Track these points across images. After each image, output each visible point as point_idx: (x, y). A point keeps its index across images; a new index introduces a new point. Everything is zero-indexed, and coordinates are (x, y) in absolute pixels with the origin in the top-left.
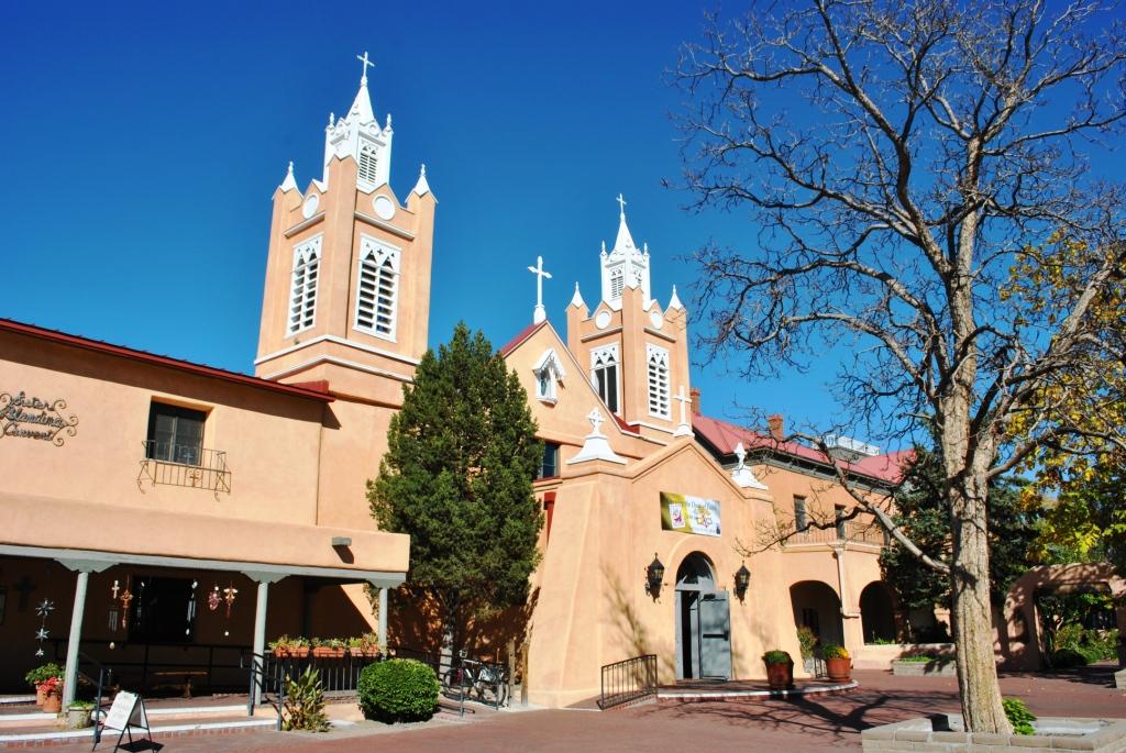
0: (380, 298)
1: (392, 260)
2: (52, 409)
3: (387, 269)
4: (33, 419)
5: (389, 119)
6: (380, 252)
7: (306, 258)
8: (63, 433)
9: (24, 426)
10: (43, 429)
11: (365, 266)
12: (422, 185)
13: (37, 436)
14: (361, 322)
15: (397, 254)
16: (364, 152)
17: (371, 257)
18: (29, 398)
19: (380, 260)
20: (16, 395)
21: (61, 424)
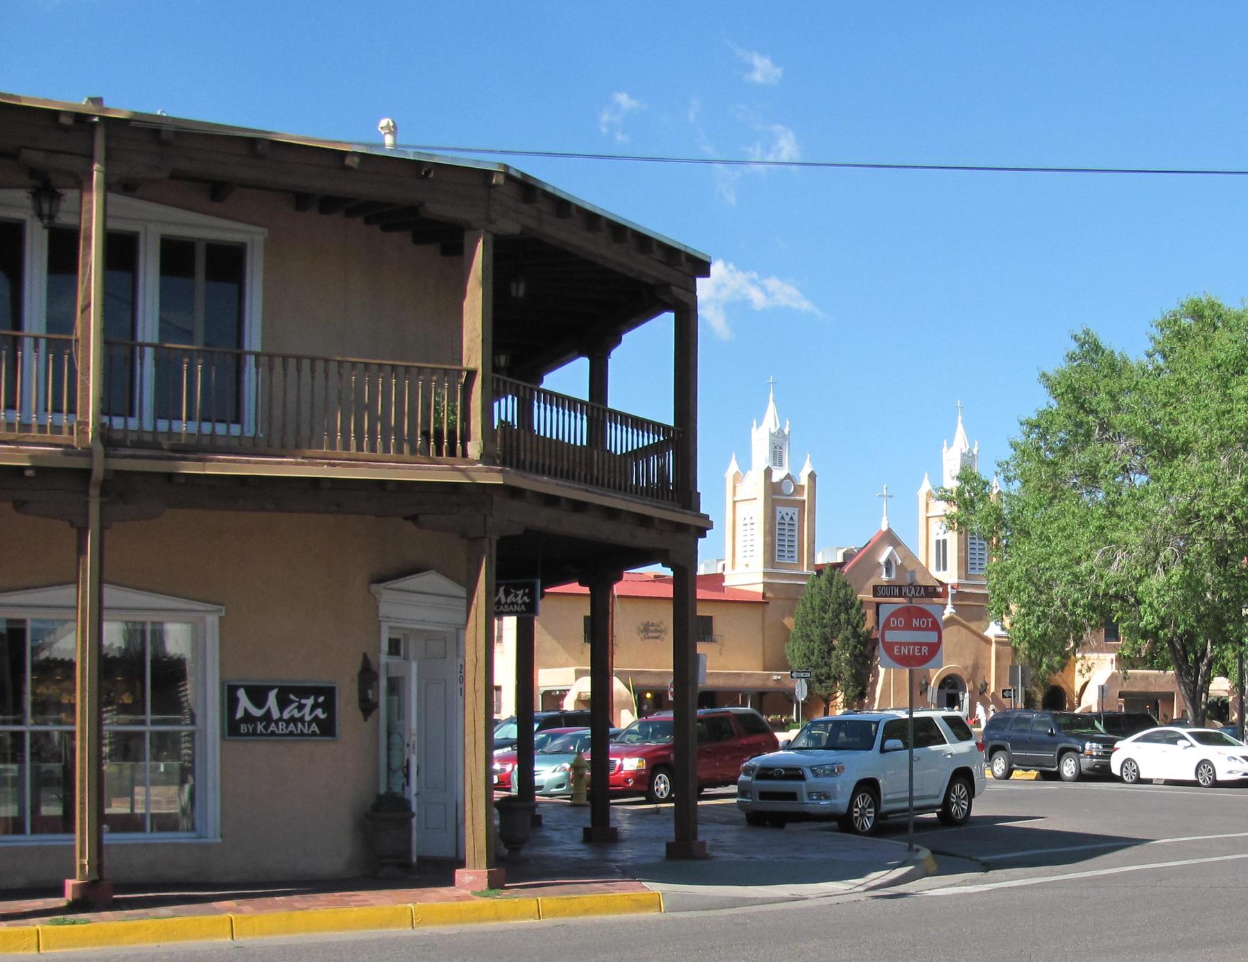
0: (788, 541)
2: (658, 626)
3: (791, 522)
4: (653, 631)
7: (748, 518)
8: (663, 635)
9: (650, 635)
10: (656, 635)
11: (779, 523)
13: (656, 638)
15: (797, 514)
17: (783, 518)
18: (650, 623)
19: (787, 519)
20: (646, 622)
21: (661, 631)
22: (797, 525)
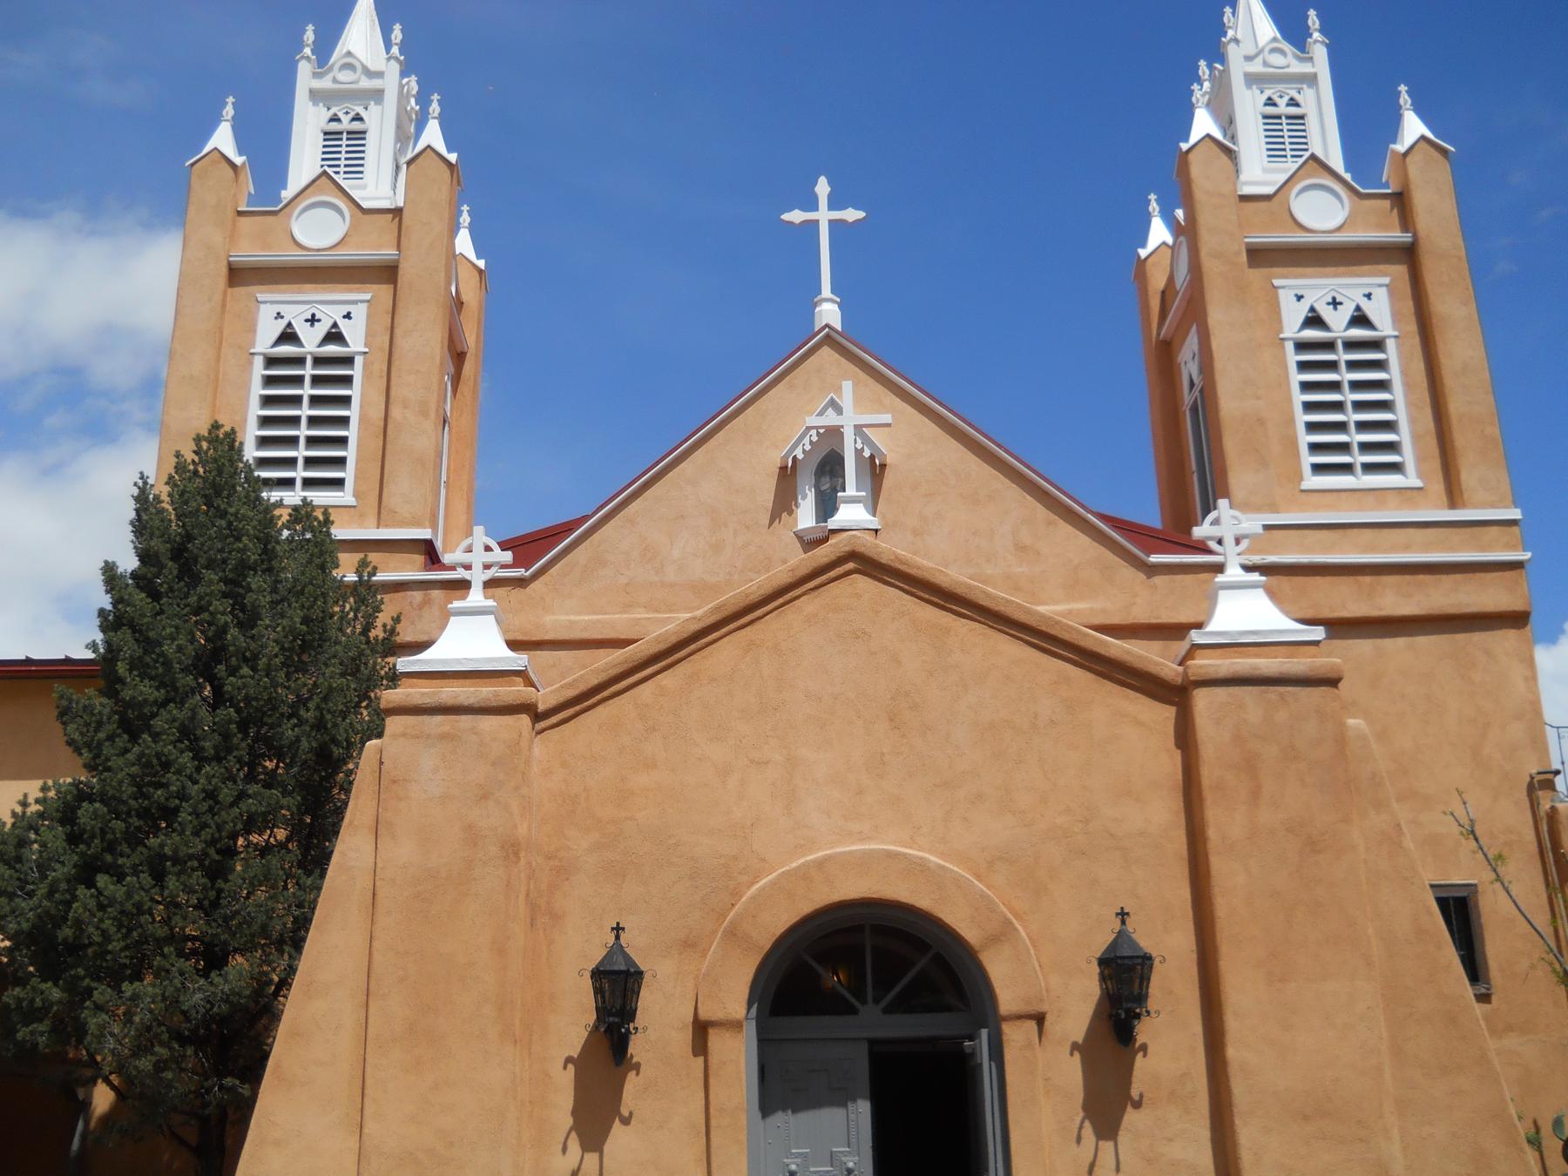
1: (1370, 309)
3: (1358, 333)
5: (1313, 19)
6: (1335, 303)
11: (1302, 346)
14: (1318, 469)
16: (1271, 110)
19: (1338, 322)
22: (1391, 345)
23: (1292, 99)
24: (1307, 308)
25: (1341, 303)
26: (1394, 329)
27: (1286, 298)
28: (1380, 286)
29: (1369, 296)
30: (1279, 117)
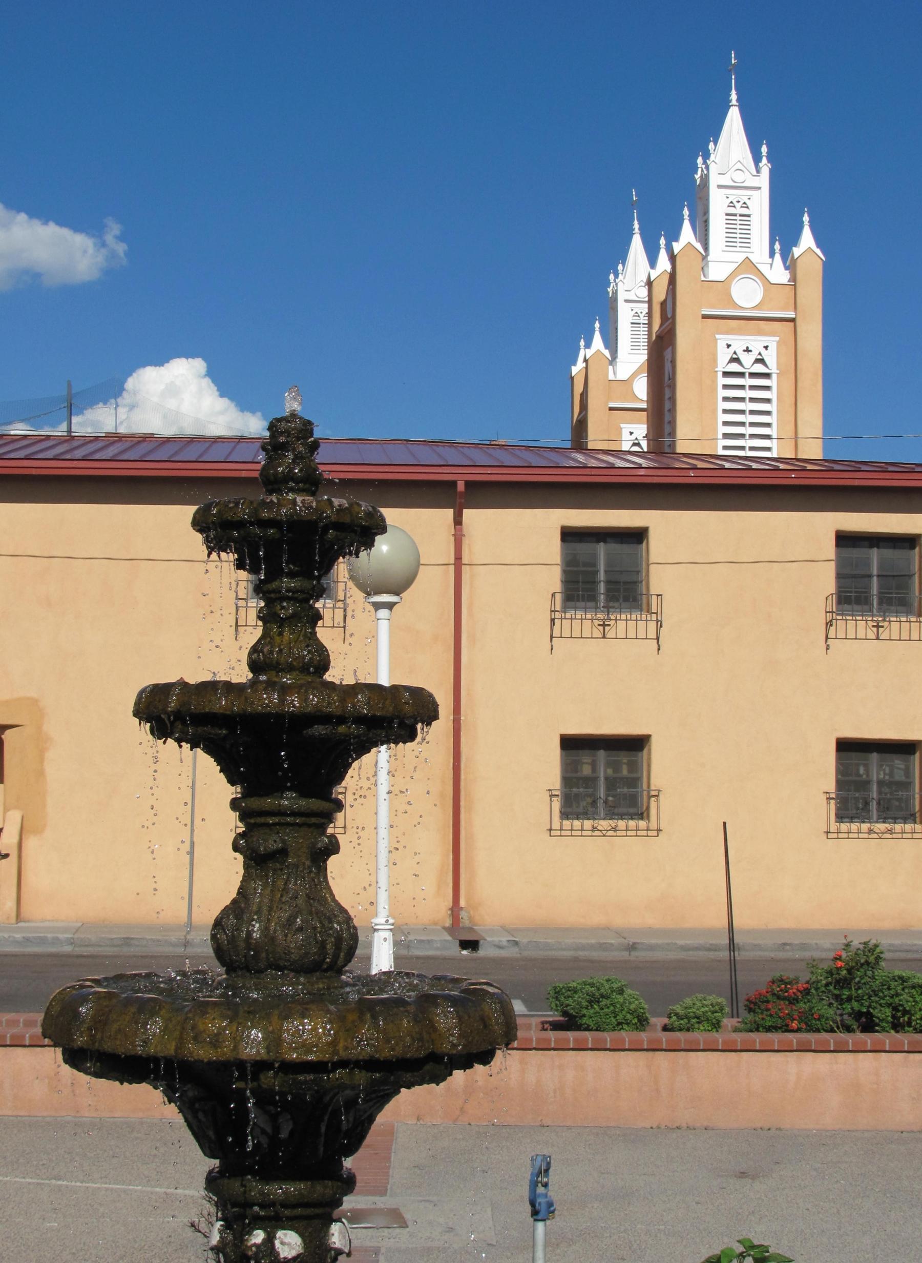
1: (766, 355)
3: (759, 368)
5: (764, 149)
6: (747, 350)
11: (726, 374)
12: (807, 239)
15: (773, 347)
16: (732, 210)
23: (745, 203)
24: (733, 352)
25: (751, 351)
26: (777, 369)
27: (721, 345)
28: (773, 341)
29: (766, 348)
30: (735, 215)
